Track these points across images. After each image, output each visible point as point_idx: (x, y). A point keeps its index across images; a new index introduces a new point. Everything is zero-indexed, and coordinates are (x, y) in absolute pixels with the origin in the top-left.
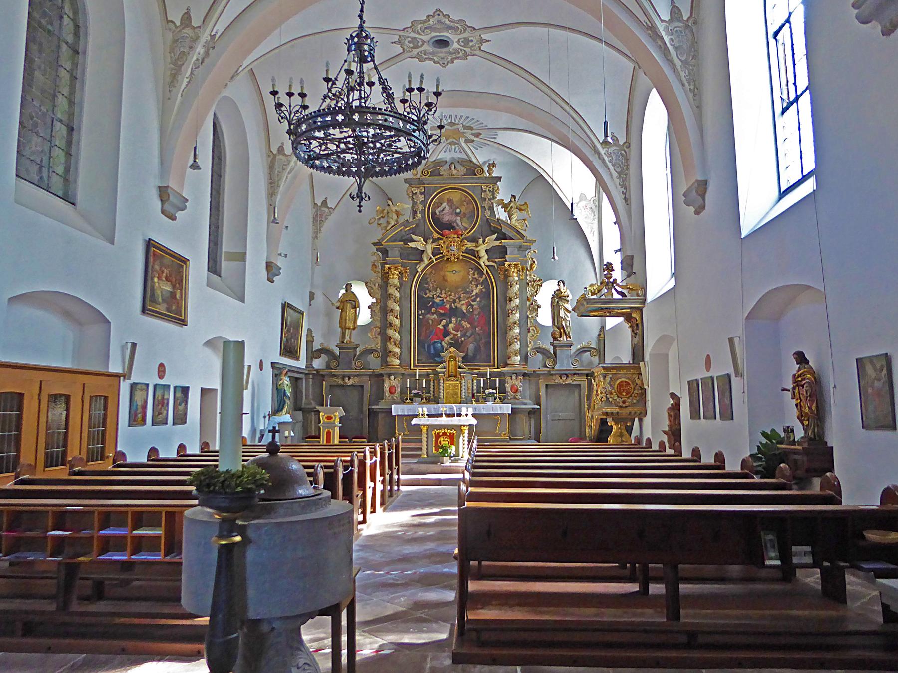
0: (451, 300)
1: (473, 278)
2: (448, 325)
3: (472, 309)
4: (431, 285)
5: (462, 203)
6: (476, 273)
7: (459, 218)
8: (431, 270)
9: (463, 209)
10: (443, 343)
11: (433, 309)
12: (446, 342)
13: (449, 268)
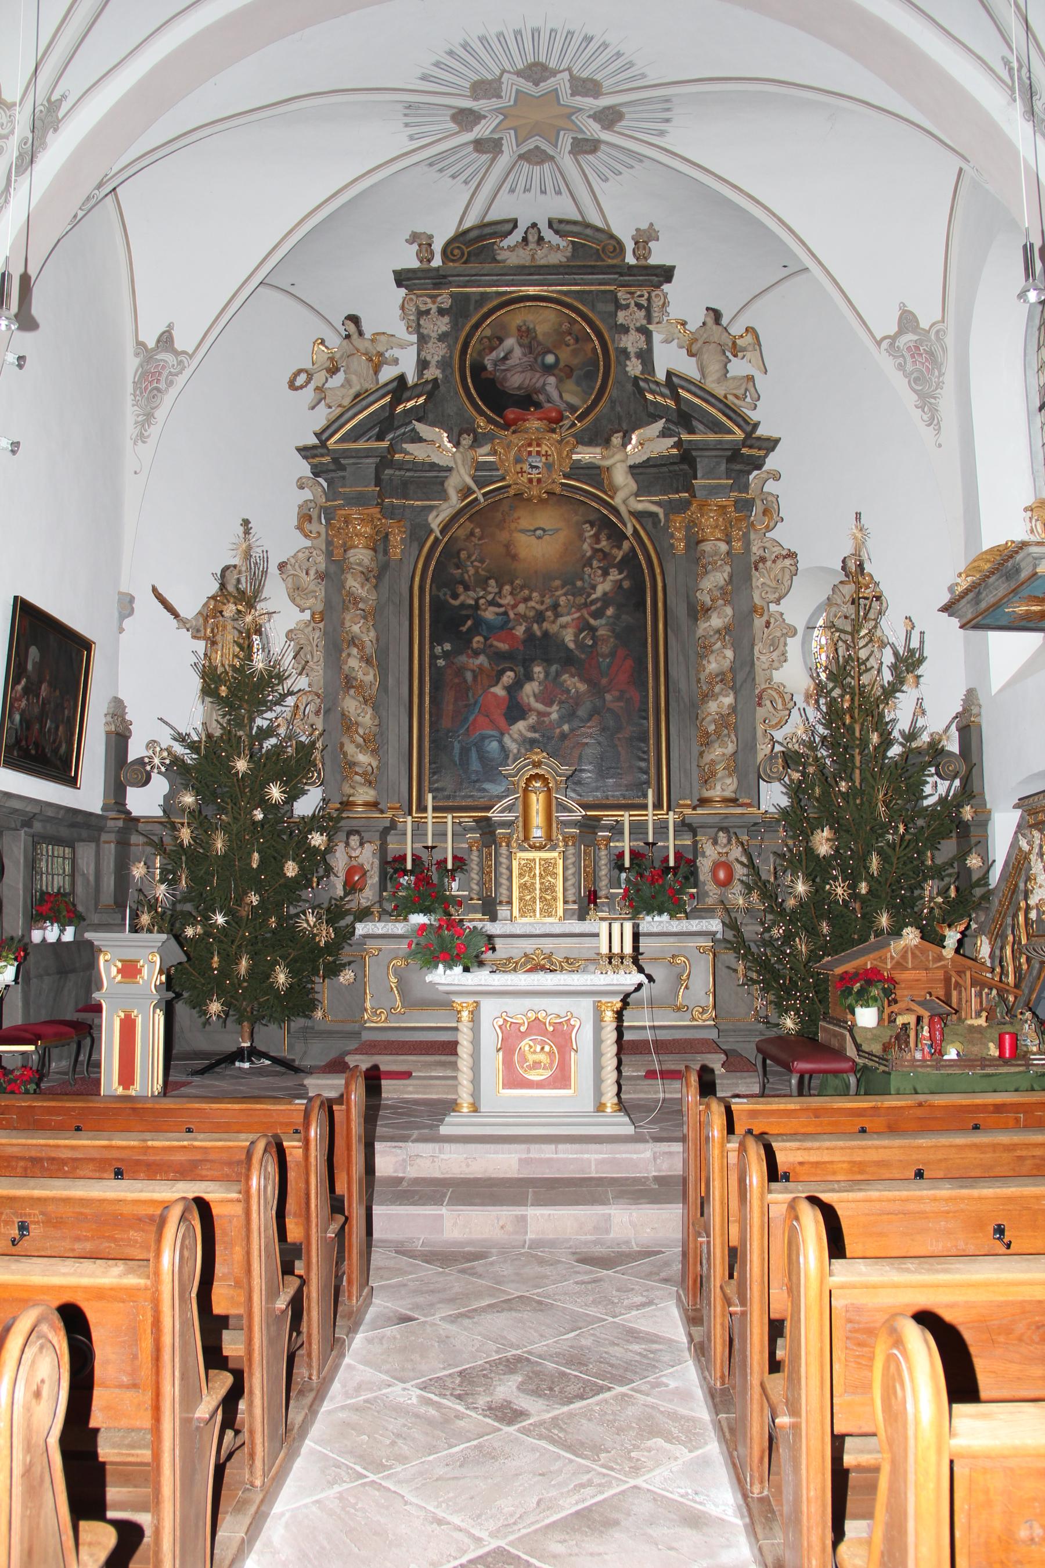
0: (532, 614)
1: (596, 551)
2: (522, 687)
3: (594, 638)
4: (472, 571)
5: (560, 336)
6: (603, 537)
7: (552, 380)
8: (469, 526)
9: (565, 355)
10: (507, 740)
11: (477, 641)
12: (516, 736)
13: (525, 523)
